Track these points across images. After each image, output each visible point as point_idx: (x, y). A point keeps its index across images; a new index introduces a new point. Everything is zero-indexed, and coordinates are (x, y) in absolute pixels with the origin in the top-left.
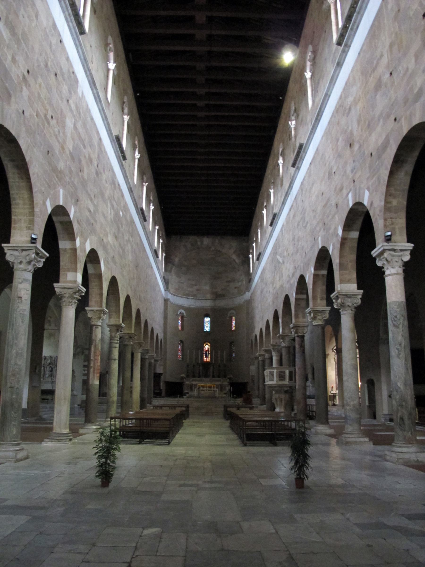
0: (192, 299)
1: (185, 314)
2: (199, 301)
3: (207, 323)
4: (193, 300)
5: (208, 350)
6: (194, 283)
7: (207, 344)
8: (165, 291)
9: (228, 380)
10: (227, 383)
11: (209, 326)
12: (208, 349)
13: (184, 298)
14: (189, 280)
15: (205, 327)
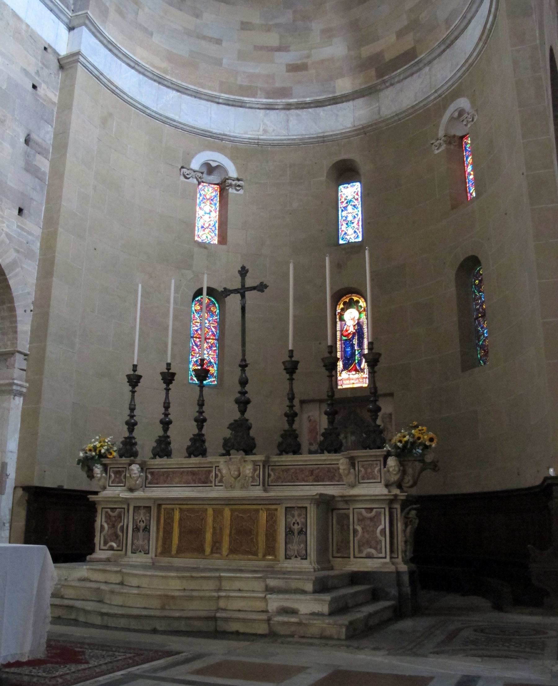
0: (269, 107)
1: (233, 172)
2: (304, 113)
3: (350, 208)
4: (272, 113)
5: (359, 332)
6: (273, 39)
7: (350, 304)
8: (71, 29)
9: (392, 462)
10: (379, 490)
11: (360, 216)
12: (359, 325)
13: (228, 103)
14: (245, 26)
15: (343, 227)
